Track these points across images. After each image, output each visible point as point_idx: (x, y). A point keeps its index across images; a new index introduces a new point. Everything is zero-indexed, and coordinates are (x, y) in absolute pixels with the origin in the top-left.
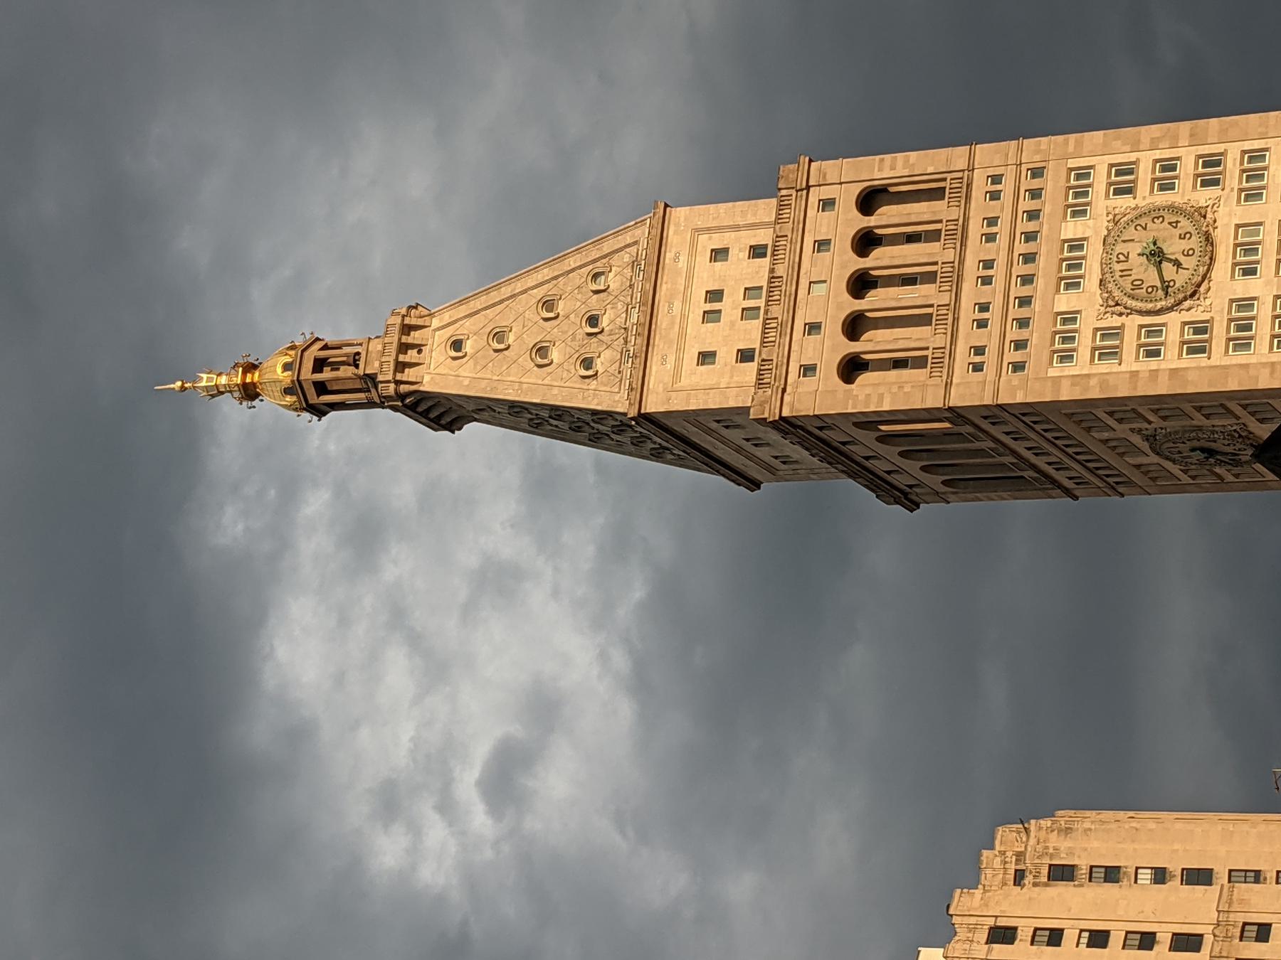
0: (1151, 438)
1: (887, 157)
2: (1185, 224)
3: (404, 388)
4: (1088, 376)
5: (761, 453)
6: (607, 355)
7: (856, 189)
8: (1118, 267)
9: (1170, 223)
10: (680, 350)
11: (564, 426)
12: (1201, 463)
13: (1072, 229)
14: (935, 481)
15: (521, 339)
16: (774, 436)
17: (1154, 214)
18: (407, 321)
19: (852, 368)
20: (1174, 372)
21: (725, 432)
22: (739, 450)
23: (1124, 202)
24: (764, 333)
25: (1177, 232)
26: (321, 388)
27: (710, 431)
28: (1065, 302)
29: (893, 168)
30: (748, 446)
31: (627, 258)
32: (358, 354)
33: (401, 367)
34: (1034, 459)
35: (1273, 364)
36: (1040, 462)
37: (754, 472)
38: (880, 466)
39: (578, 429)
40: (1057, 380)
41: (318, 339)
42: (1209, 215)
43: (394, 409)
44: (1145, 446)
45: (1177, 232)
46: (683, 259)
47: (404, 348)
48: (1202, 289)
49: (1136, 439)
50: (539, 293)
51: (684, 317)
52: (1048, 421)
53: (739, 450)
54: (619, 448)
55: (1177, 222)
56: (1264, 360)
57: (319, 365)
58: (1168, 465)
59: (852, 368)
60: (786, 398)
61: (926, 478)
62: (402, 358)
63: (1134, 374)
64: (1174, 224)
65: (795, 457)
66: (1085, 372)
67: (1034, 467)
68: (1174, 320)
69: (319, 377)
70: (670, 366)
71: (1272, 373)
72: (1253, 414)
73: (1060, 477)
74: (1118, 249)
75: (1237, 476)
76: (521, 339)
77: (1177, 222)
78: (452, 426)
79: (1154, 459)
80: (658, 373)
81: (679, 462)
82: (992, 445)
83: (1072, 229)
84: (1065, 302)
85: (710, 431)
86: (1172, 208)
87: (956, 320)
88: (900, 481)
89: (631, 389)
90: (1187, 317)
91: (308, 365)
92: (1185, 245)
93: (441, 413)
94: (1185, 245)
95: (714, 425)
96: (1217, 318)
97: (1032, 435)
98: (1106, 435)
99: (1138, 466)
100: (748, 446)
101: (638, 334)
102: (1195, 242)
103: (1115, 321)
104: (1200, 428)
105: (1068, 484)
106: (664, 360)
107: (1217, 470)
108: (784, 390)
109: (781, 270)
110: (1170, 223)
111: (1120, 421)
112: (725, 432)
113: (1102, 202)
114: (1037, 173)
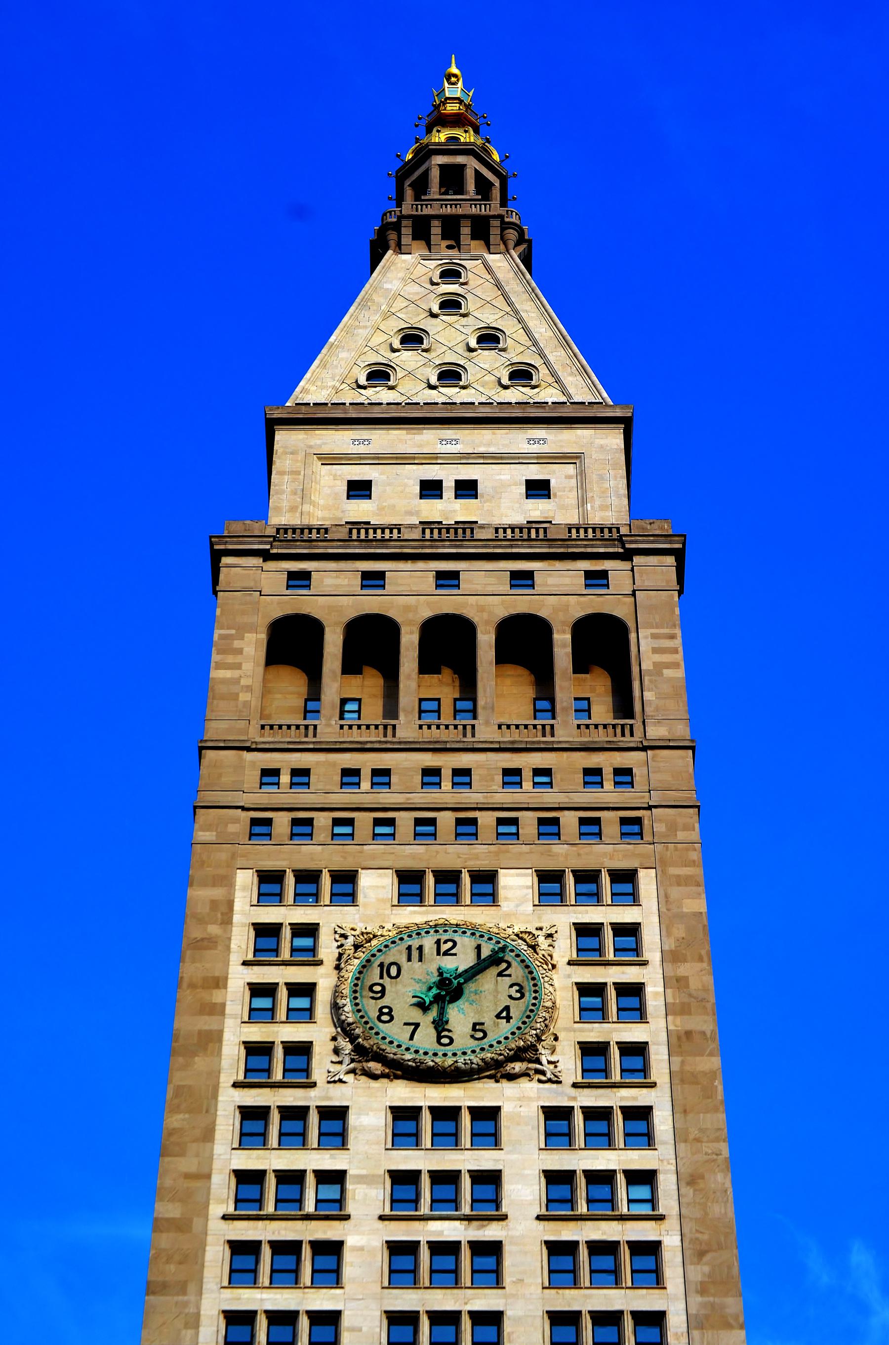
1: (678, 642)
4: (227, 920)
8: (428, 943)
9: (507, 1008)
10: (378, 459)
13: (517, 885)
17: (528, 986)
18: (496, 223)
20: (215, 1038)
23: (564, 947)
25: (488, 1019)
28: (377, 886)
29: (655, 651)
35: (208, 1177)
40: (227, 882)
42: (518, 1067)
48: (375, 1067)
51: (433, 459)
55: (508, 1018)
56: (216, 1165)
63: (220, 982)
64: (505, 1014)
66: (236, 918)
71: (188, 1176)
77: (508, 1018)
83: (517, 885)
84: (377, 886)
96: (312, 1093)
103: (327, 949)
108: (267, 556)
110: (507, 1008)
113: (563, 919)
114: (632, 827)
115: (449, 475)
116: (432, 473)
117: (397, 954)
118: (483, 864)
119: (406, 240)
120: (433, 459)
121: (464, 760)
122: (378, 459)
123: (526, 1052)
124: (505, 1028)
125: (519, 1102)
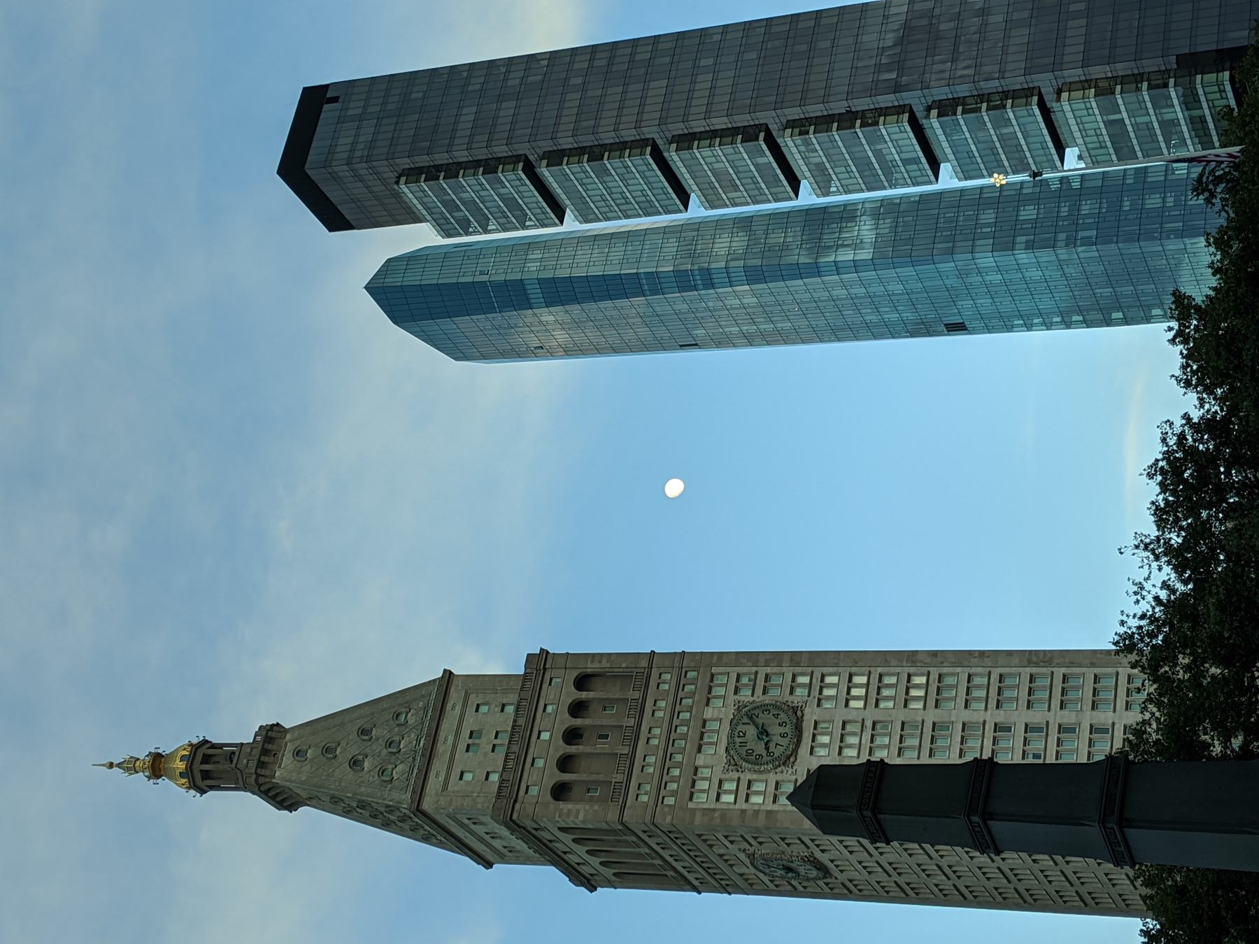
0: (751, 857)
2: (783, 716)
3: (261, 780)
4: (714, 810)
5: (497, 844)
6: (400, 767)
7: (575, 674)
8: (738, 740)
10: (450, 768)
11: (366, 813)
12: (782, 877)
14: (608, 872)
15: (345, 753)
16: (505, 832)
19: (560, 792)
20: (769, 812)
21: (473, 827)
22: (481, 840)
24: (505, 761)
25: (778, 721)
26: (206, 775)
27: (462, 825)
30: (487, 837)
31: (421, 704)
32: (233, 753)
33: (261, 765)
34: (674, 864)
36: (678, 866)
37: (489, 856)
38: (573, 859)
39: (375, 817)
41: (207, 742)
42: (799, 713)
43: (254, 793)
44: (747, 861)
45: (778, 721)
46: (458, 708)
47: (265, 752)
49: (742, 856)
50: (360, 723)
51: (454, 747)
52: (686, 838)
53: (481, 840)
54: (401, 832)
57: (206, 759)
58: (761, 875)
59: (560, 792)
60: (517, 806)
61: (602, 870)
62: (263, 758)
63: (743, 811)
64: (776, 716)
65: (518, 848)
67: (674, 869)
68: (772, 778)
69: (206, 767)
70: (441, 778)
72: (818, 846)
73: (691, 877)
74: (739, 728)
75: (805, 887)
76: (345, 753)
78: (291, 807)
79: (753, 870)
80: (434, 783)
81: (440, 845)
82: (647, 851)
85: (462, 825)
86: (775, 706)
87: (632, 765)
88: (585, 870)
89: (414, 792)
90: (779, 777)
91: (199, 758)
92: (781, 730)
93: (285, 800)
94: (781, 730)
95: (466, 821)
97: (674, 846)
98: (722, 851)
99: (741, 875)
100: (487, 837)
101: (423, 755)
102: (788, 729)
104: (783, 853)
105: (696, 883)
106: (437, 776)
107: (793, 882)
108: (515, 801)
109: (521, 721)
111: (732, 842)
112: (473, 827)
115: (464, 740)
116: (462, 747)
117: (743, 751)
118: (700, 724)
119: (267, 772)
120: (454, 747)
121: (644, 728)
122: (450, 768)
123: (795, 710)
124: (783, 715)
125: (811, 714)
